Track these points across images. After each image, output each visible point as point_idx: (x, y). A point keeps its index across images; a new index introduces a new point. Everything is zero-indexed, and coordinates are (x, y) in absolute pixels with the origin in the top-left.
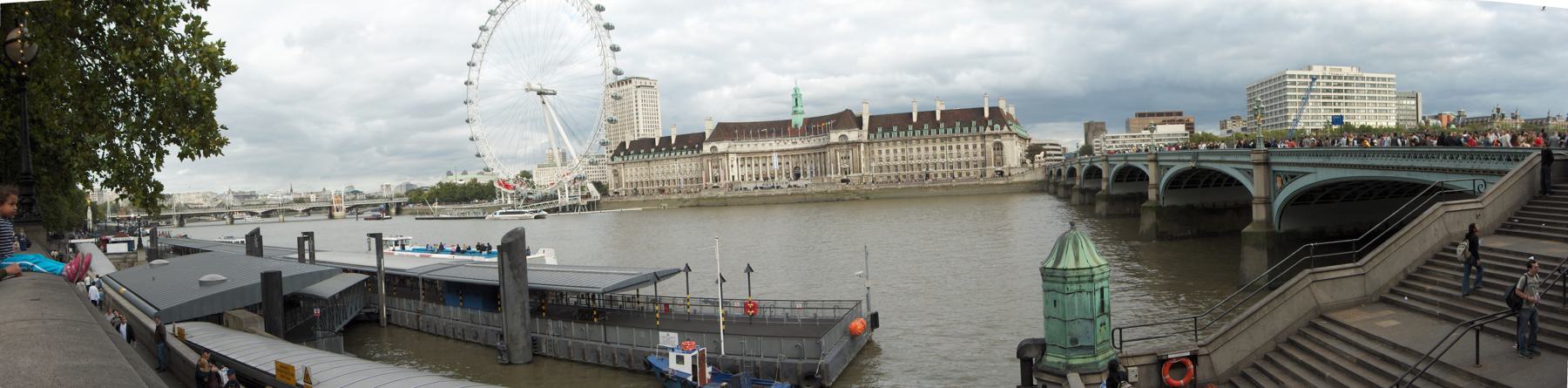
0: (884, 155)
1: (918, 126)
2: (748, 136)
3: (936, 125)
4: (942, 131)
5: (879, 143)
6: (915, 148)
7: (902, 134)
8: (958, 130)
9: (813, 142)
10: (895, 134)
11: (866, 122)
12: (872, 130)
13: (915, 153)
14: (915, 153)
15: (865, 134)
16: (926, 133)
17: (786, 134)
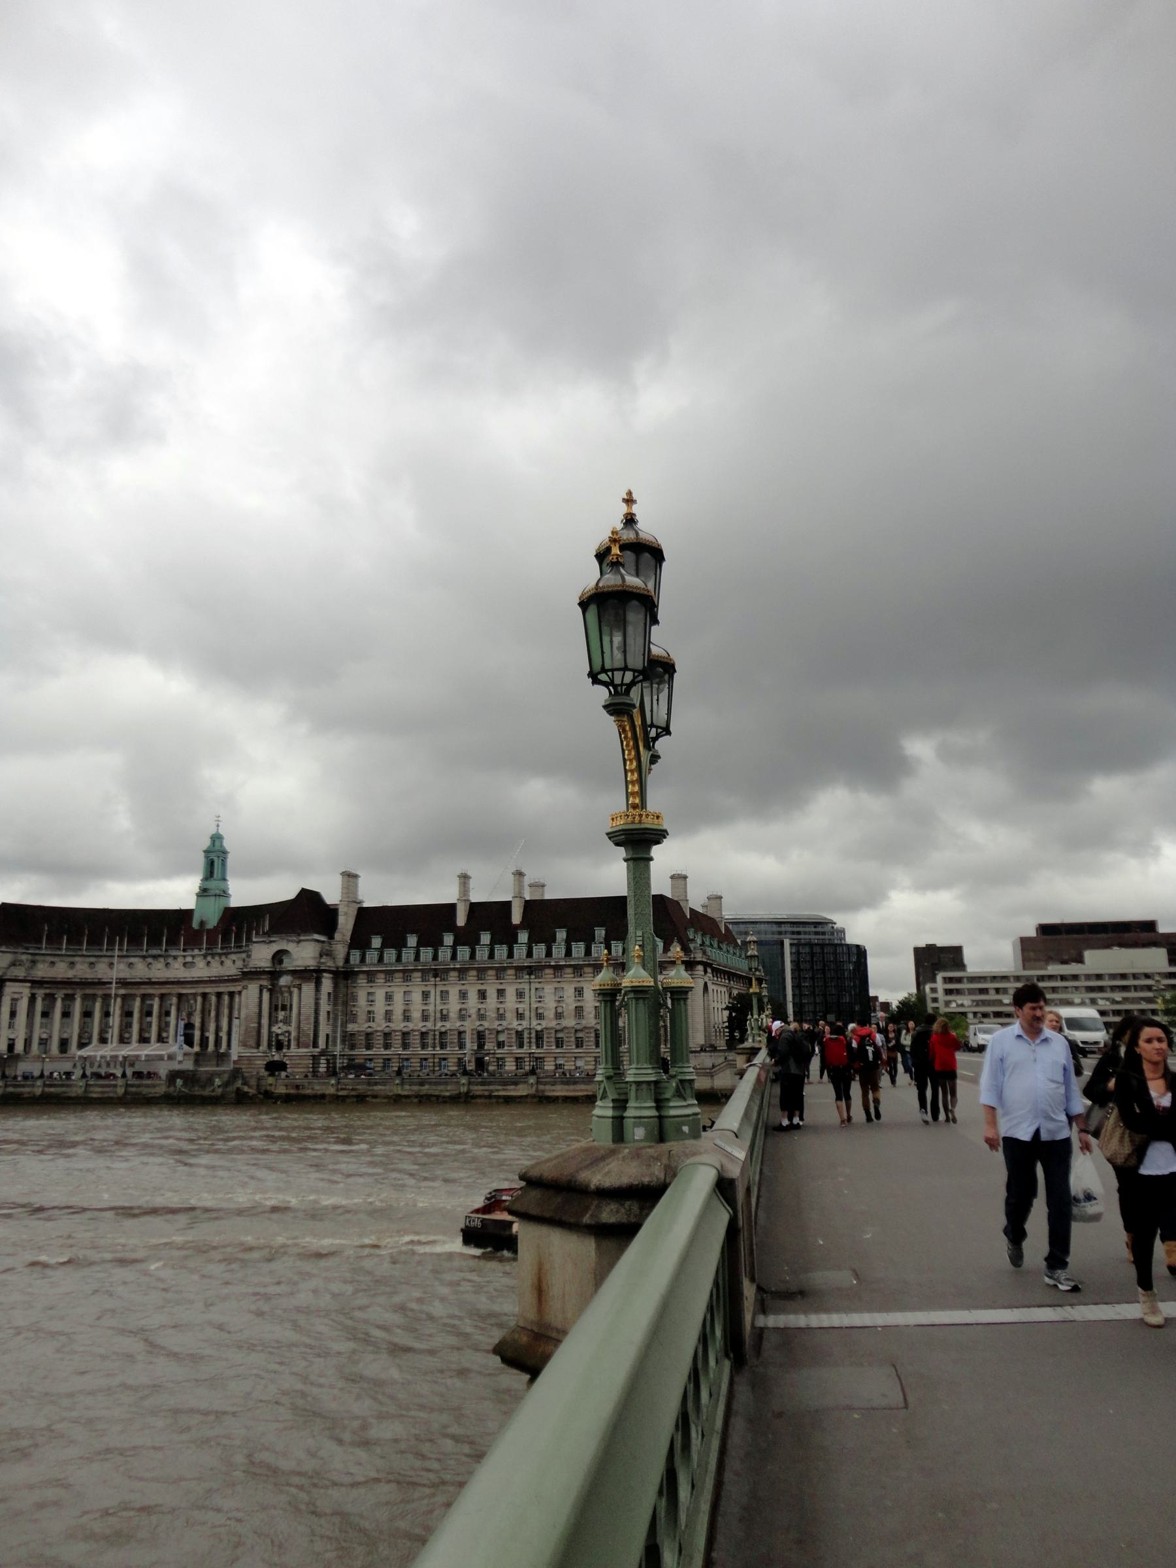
0: (380, 1007)
1: (467, 937)
2: (74, 941)
3: (506, 935)
4: (520, 952)
5: (371, 976)
6: (454, 993)
7: (426, 954)
8: (559, 951)
9: (230, 966)
10: (408, 955)
11: (346, 923)
12: (359, 941)
13: (454, 1005)
14: (454, 1005)
15: (340, 950)
16: (482, 954)
17: (173, 942)
